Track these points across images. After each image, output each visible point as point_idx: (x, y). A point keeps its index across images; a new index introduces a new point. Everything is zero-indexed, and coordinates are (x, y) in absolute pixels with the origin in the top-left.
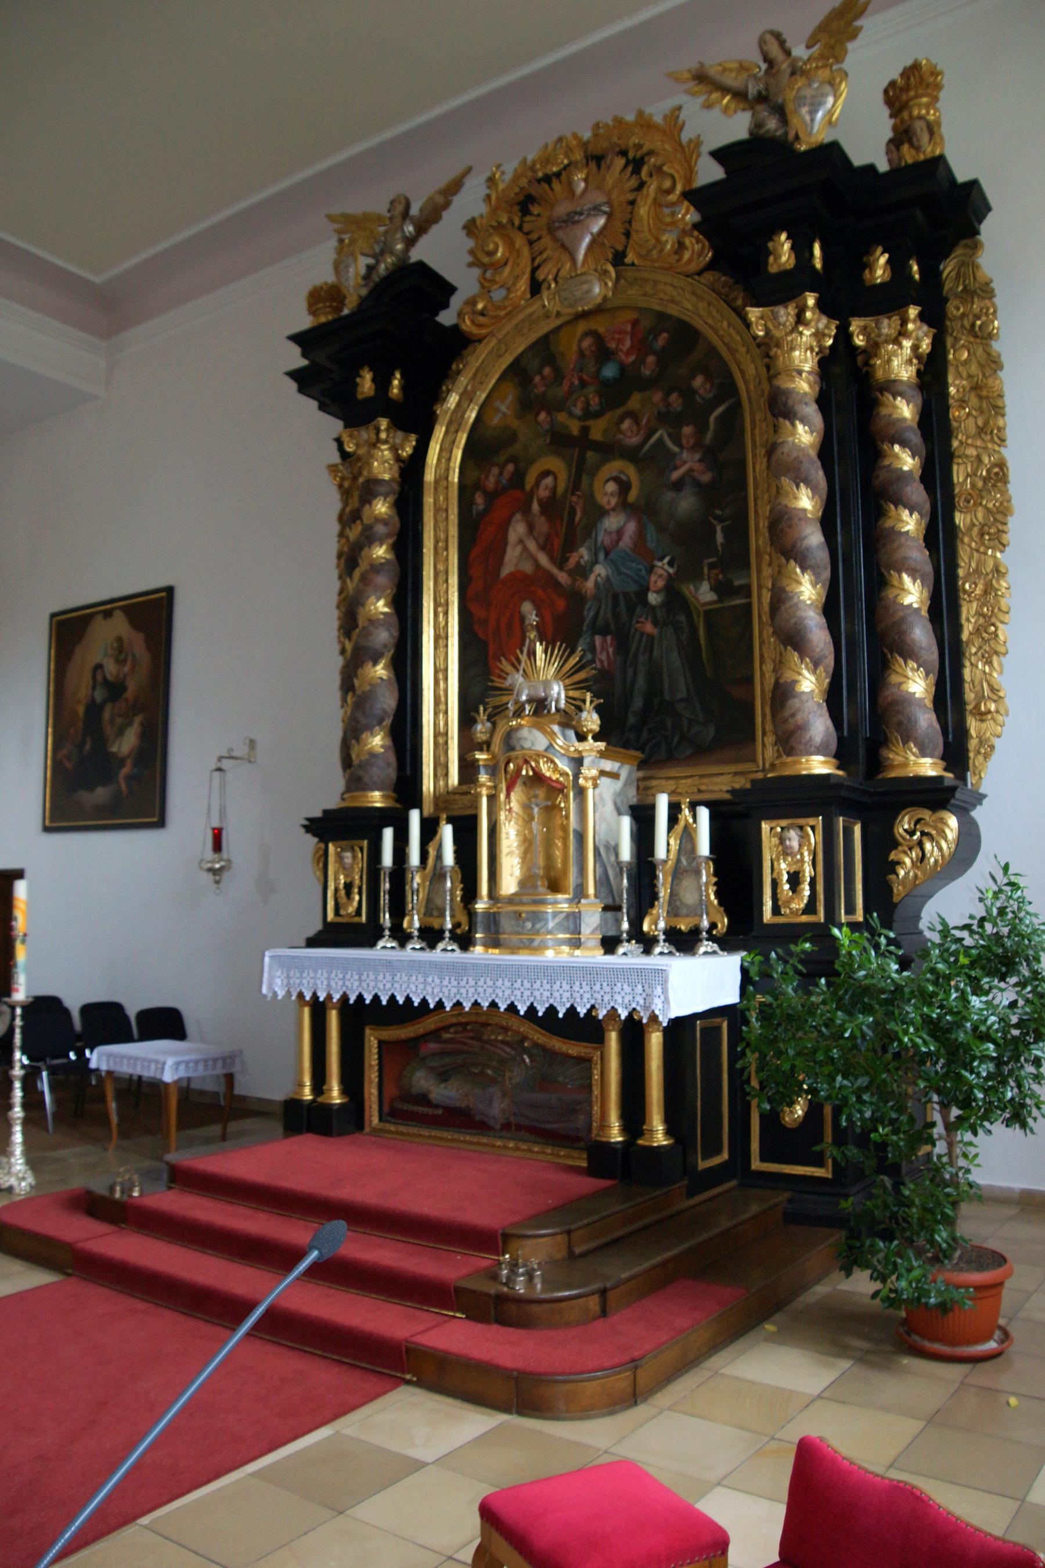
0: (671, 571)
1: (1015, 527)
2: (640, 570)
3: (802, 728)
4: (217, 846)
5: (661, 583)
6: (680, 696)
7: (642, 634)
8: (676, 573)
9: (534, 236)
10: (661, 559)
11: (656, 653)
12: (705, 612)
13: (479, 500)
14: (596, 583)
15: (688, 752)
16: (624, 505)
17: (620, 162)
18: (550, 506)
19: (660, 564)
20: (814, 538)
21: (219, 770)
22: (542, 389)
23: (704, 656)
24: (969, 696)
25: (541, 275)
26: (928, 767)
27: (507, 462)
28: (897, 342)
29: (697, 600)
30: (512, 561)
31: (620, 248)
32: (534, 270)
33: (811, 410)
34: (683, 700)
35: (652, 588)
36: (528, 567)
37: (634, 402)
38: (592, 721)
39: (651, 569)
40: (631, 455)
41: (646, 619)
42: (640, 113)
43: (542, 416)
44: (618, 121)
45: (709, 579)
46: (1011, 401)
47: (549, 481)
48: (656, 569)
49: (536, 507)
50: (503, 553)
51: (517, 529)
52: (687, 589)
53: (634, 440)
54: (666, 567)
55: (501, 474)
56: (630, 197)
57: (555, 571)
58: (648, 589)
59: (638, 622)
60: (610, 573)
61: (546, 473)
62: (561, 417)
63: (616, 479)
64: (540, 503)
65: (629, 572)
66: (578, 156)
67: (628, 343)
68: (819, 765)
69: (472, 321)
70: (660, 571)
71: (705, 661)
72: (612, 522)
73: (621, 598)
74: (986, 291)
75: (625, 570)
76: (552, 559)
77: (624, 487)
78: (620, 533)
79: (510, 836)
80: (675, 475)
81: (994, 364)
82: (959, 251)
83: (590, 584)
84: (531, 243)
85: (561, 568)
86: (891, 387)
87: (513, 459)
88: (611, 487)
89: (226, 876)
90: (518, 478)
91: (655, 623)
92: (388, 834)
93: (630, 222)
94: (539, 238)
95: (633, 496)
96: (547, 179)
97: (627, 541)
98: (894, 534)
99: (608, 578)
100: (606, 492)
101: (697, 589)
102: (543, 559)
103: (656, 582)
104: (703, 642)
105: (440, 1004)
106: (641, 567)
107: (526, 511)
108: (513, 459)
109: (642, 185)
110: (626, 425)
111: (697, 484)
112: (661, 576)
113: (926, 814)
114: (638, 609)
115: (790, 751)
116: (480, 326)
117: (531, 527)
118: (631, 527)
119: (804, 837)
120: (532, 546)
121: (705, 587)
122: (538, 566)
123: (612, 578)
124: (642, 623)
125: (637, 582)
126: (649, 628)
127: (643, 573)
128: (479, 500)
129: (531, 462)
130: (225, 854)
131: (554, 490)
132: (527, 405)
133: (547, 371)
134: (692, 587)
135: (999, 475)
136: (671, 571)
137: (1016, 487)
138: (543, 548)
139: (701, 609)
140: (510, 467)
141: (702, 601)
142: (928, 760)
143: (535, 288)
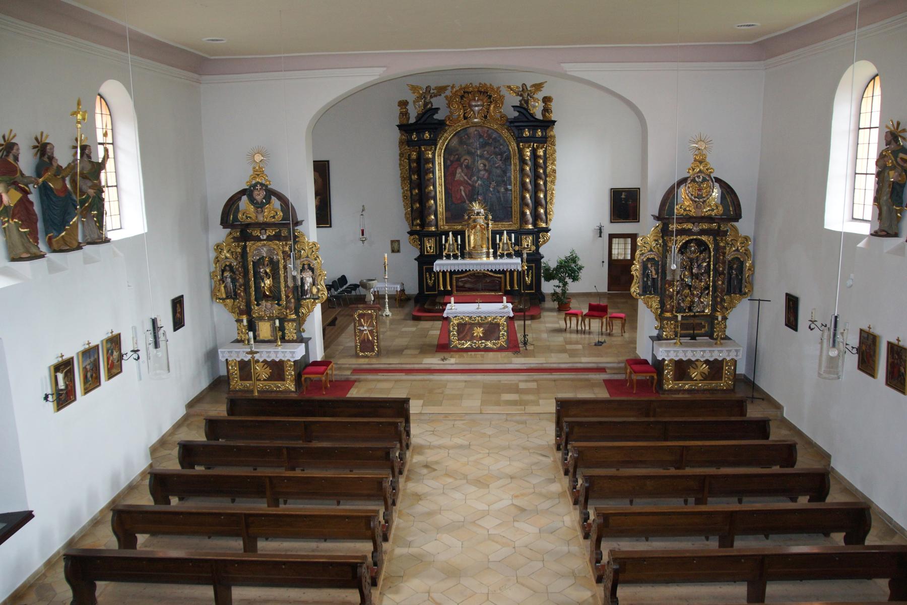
1: (557, 182)
3: (528, 220)
4: (363, 234)
5: (493, 187)
9: (464, 105)
13: (449, 162)
14: (478, 185)
16: (485, 170)
17: (486, 95)
18: (467, 167)
20: (529, 187)
21: (362, 215)
22: (465, 140)
24: (548, 211)
25: (466, 115)
26: (544, 225)
27: (456, 155)
28: (542, 149)
30: (458, 176)
31: (486, 114)
32: (465, 114)
33: (529, 163)
36: (462, 179)
37: (487, 148)
38: (490, 217)
39: (490, 183)
40: (487, 159)
42: (491, 85)
43: (465, 146)
44: (485, 84)
46: (557, 158)
47: (467, 161)
49: (464, 166)
50: (456, 175)
51: (459, 170)
52: (499, 188)
53: (488, 156)
55: (454, 157)
56: (489, 103)
57: (469, 181)
61: (466, 159)
62: (469, 147)
63: (484, 164)
64: (464, 165)
66: (476, 90)
67: (485, 135)
68: (530, 227)
69: (449, 123)
72: (482, 173)
74: (554, 137)
76: (468, 178)
77: (485, 165)
78: (484, 175)
79: (472, 238)
80: (497, 165)
81: (555, 151)
82: (550, 128)
83: (477, 184)
84: (463, 107)
85: (470, 180)
86: (540, 157)
87: (457, 154)
88: (482, 165)
89: (365, 241)
90: (458, 160)
91: (492, 194)
92: (444, 237)
93: (488, 109)
94: (466, 106)
95: (487, 168)
96: (468, 93)
97: (485, 177)
98: (539, 183)
100: (481, 167)
102: (466, 178)
105: (470, 270)
107: (461, 166)
108: (457, 154)
109: (491, 102)
110: (485, 153)
111: (501, 167)
113: (545, 233)
115: (526, 224)
116: (451, 124)
117: (462, 171)
118: (487, 174)
119: (529, 238)
120: (463, 174)
121: (503, 188)
122: (464, 178)
126: (490, 195)
128: (449, 162)
129: (462, 157)
130: (365, 236)
131: (468, 163)
132: (461, 142)
133: (466, 136)
135: (554, 171)
137: (557, 175)
138: (466, 175)
140: (457, 156)
142: (544, 224)
143: (465, 118)
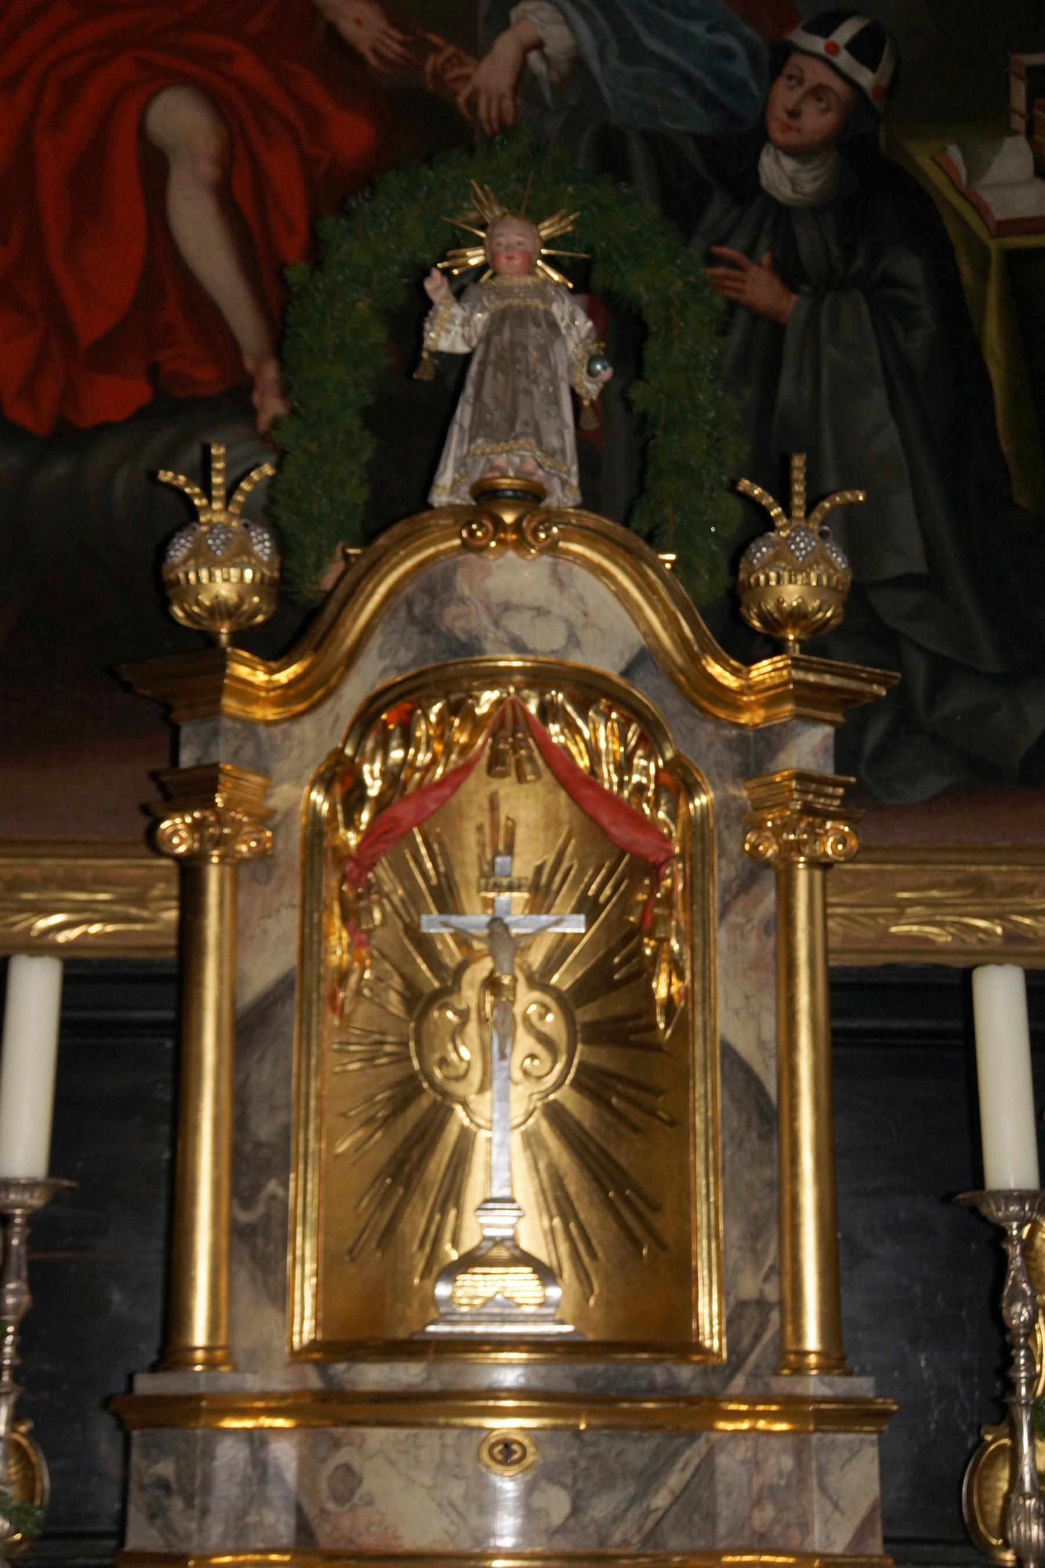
0: (866, 78)
2: (728, 55)
6: (894, 567)
7: (733, 306)
8: (889, 92)
10: (824, 26)
11: (786, 388)
12: (1011, 257)
14: (523, 77)
15: (933, 784)
19: (818, 44)
23: (1001, 425)
29: (980, 209)
34: (908, 581)
35: (776, 133)
41: (750, 252)
45: (1029, 134)
48: (797, 60)
54: (843, 60)
58: (761, 137)
59: (712, 260)
60: (589, 46)
65: (672, 55)
70: (817, 74)
71: (1006, 448)
73: (637, 153)
75: (655, 45)
99: (578, 61)
101: (976, 167)
103: (794, 114)
104: (996, 373)
106: (731, 42)
112: (818, 92)
114: (716, 209)
123: (594, 65)
124: (733, 265)
125: (709, 101)
127: (741, 68)
134: (954, 153)
136: (866, 78)
139: (994, 245)
141: (999, 215)
